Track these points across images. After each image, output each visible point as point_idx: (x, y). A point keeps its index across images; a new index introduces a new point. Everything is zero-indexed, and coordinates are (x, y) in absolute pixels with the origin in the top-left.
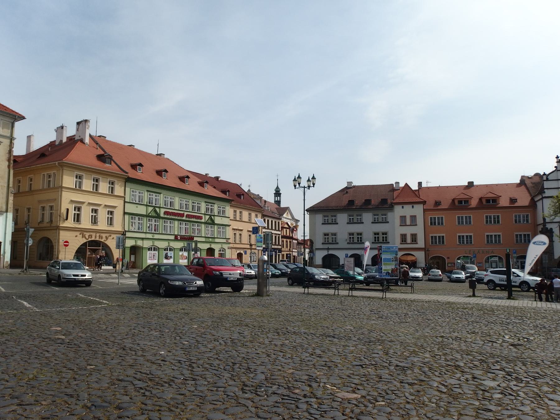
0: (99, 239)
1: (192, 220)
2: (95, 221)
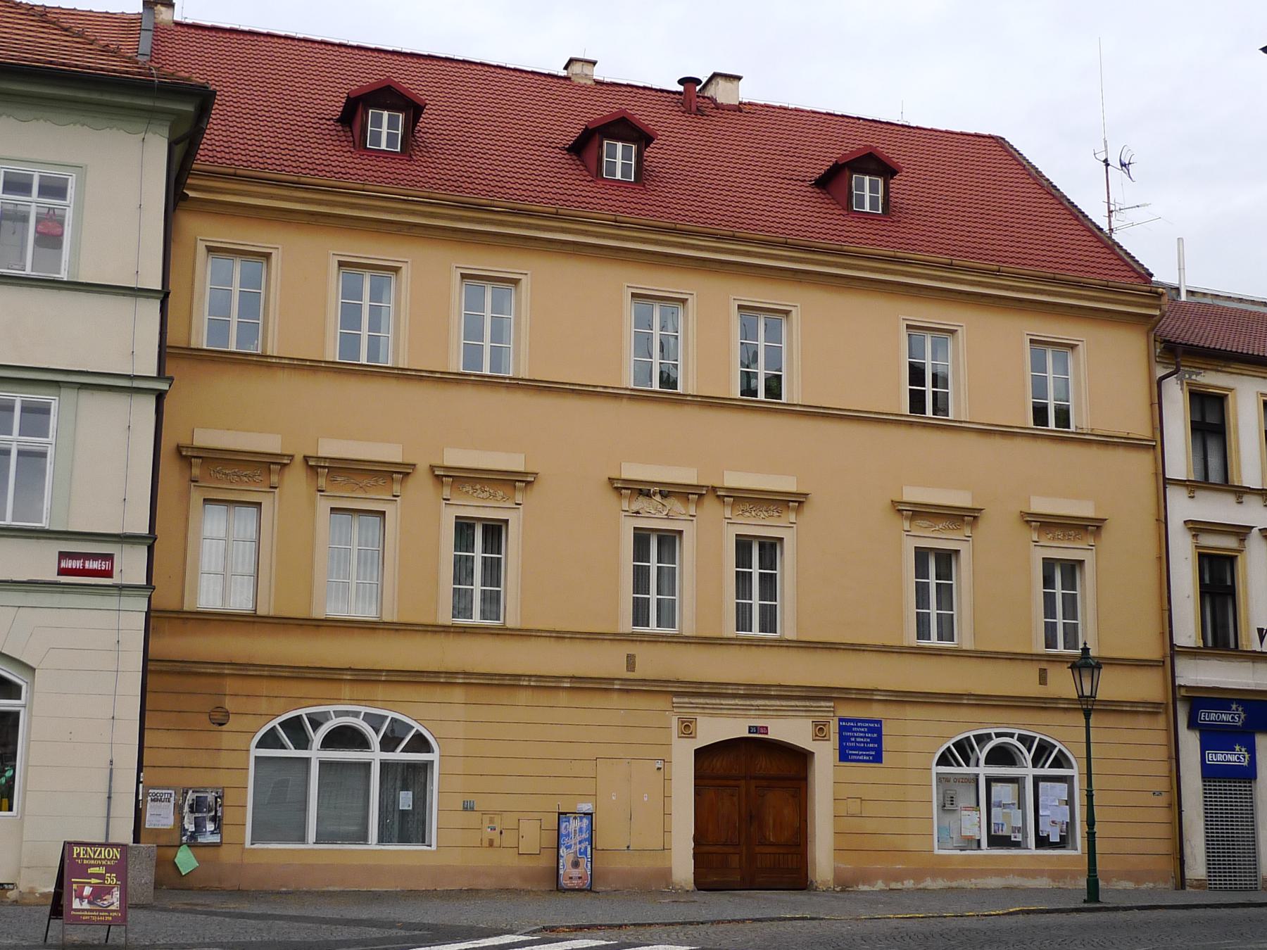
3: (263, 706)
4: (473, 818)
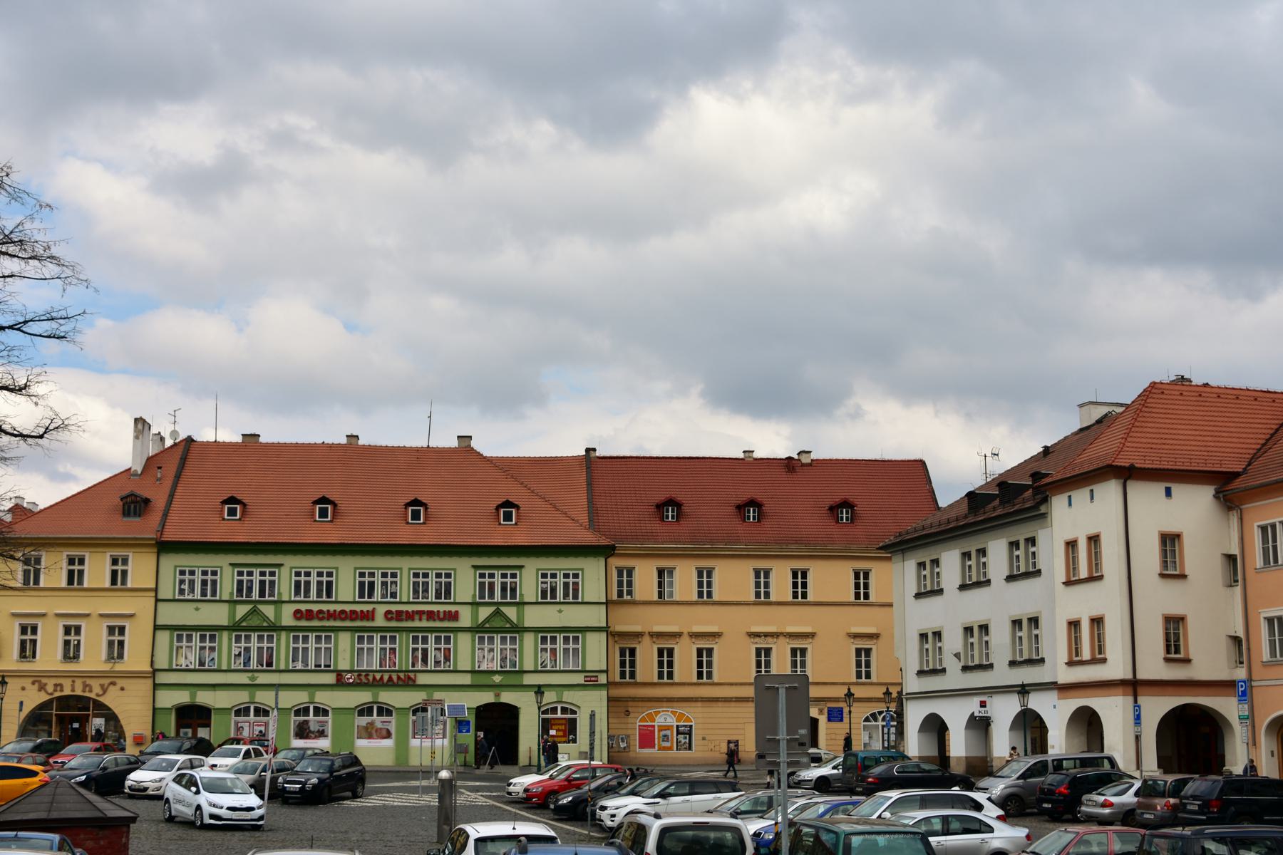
0: (84, 691)
1: (416, 624)
2: (71, 652)
3: (640, 710)
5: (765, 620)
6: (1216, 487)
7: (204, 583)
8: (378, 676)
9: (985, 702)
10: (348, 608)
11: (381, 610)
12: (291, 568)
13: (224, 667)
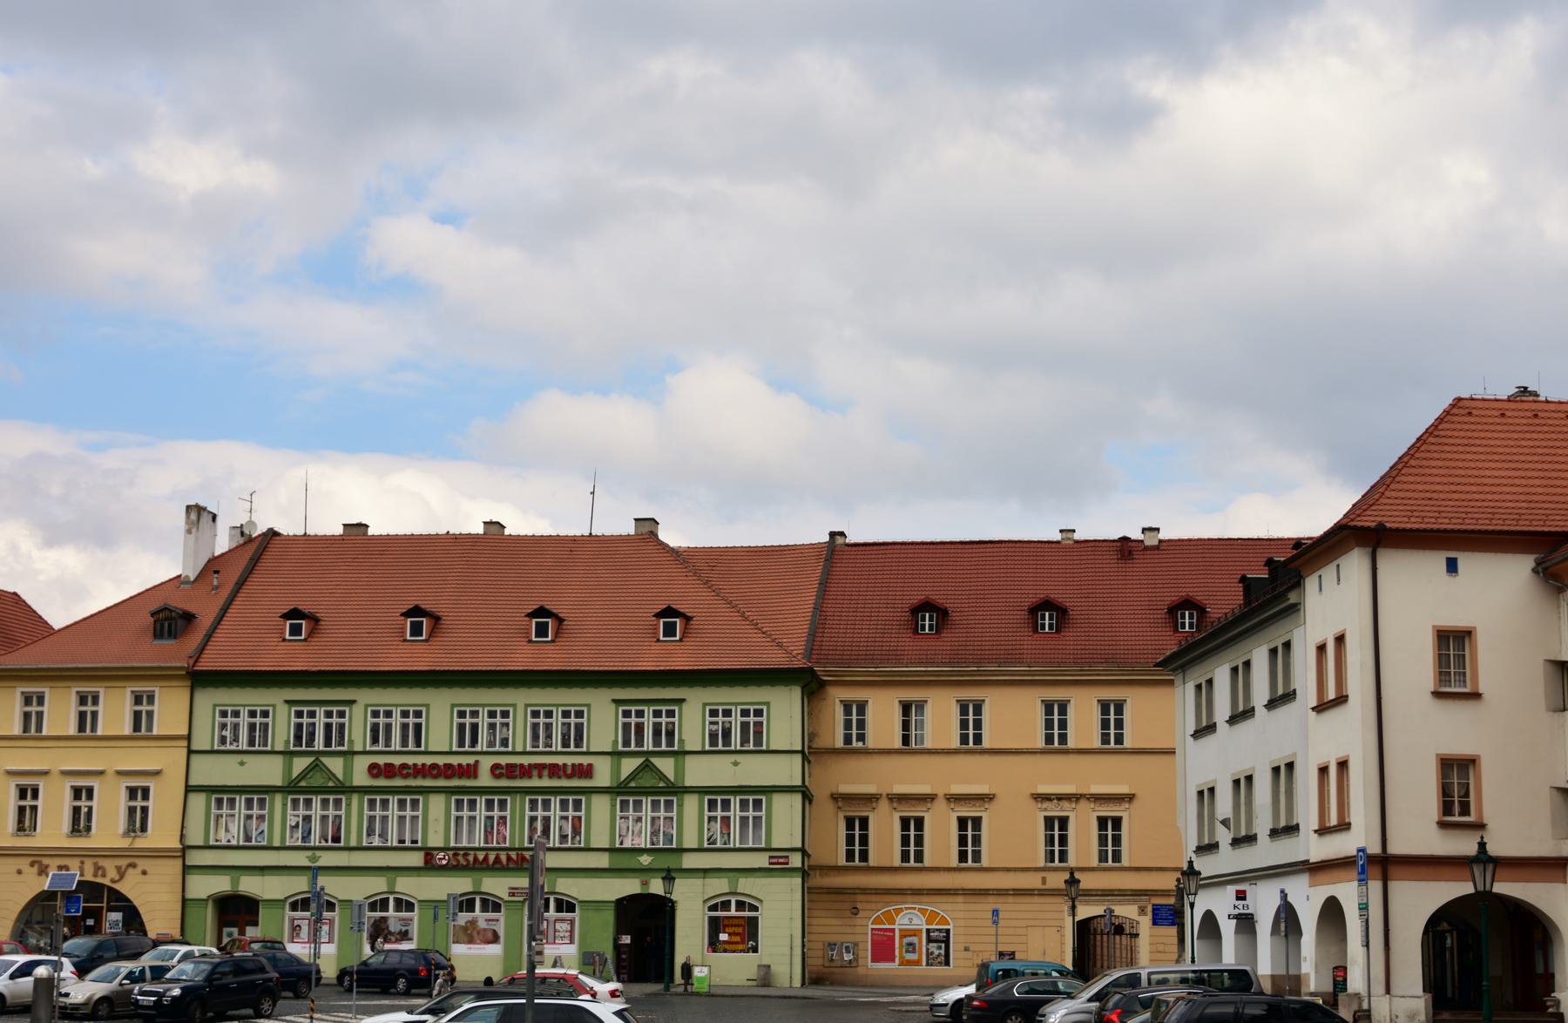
0: (95, 875)
1: (535, 782)
2: (80, 822)
3: (873, 906)
4: (969, 954)
5: (1060, 776)
6: (1534, 556)
7: (252, 727)
8: (481, 856)
9: (1244, 892)
10: (441, 761)
11: (486, 763)
12: (367, 706)
13: (277, 843)
